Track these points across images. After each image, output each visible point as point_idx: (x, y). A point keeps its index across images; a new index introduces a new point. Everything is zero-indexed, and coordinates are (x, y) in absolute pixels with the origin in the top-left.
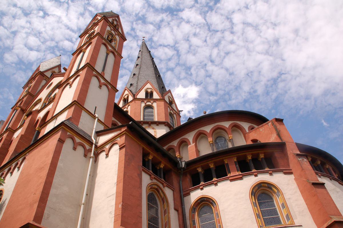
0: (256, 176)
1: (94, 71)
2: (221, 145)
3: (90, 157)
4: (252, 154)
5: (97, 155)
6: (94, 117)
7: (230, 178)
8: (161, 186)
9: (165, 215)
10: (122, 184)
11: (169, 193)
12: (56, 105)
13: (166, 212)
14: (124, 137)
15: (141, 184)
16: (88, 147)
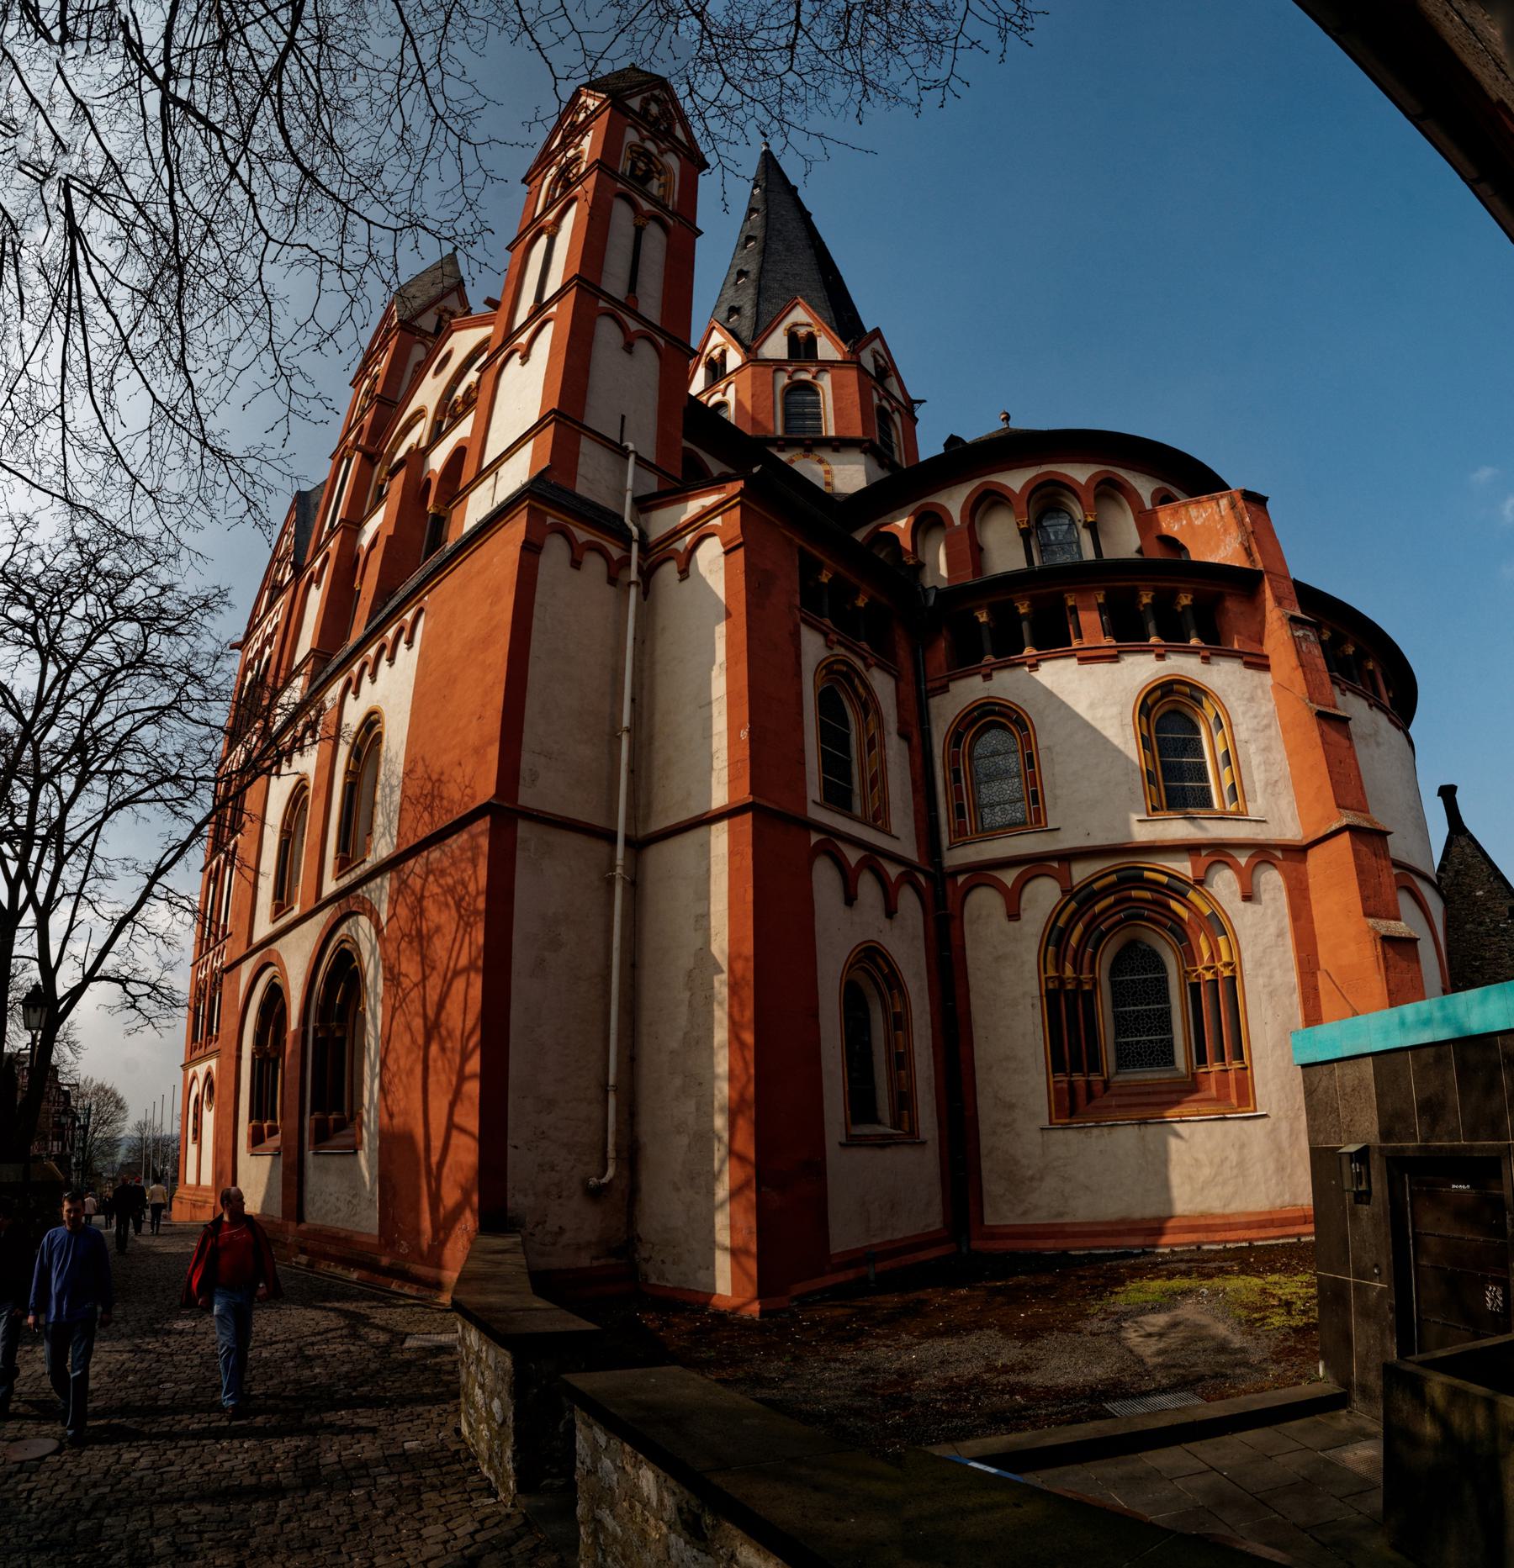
2: (1056, 537)
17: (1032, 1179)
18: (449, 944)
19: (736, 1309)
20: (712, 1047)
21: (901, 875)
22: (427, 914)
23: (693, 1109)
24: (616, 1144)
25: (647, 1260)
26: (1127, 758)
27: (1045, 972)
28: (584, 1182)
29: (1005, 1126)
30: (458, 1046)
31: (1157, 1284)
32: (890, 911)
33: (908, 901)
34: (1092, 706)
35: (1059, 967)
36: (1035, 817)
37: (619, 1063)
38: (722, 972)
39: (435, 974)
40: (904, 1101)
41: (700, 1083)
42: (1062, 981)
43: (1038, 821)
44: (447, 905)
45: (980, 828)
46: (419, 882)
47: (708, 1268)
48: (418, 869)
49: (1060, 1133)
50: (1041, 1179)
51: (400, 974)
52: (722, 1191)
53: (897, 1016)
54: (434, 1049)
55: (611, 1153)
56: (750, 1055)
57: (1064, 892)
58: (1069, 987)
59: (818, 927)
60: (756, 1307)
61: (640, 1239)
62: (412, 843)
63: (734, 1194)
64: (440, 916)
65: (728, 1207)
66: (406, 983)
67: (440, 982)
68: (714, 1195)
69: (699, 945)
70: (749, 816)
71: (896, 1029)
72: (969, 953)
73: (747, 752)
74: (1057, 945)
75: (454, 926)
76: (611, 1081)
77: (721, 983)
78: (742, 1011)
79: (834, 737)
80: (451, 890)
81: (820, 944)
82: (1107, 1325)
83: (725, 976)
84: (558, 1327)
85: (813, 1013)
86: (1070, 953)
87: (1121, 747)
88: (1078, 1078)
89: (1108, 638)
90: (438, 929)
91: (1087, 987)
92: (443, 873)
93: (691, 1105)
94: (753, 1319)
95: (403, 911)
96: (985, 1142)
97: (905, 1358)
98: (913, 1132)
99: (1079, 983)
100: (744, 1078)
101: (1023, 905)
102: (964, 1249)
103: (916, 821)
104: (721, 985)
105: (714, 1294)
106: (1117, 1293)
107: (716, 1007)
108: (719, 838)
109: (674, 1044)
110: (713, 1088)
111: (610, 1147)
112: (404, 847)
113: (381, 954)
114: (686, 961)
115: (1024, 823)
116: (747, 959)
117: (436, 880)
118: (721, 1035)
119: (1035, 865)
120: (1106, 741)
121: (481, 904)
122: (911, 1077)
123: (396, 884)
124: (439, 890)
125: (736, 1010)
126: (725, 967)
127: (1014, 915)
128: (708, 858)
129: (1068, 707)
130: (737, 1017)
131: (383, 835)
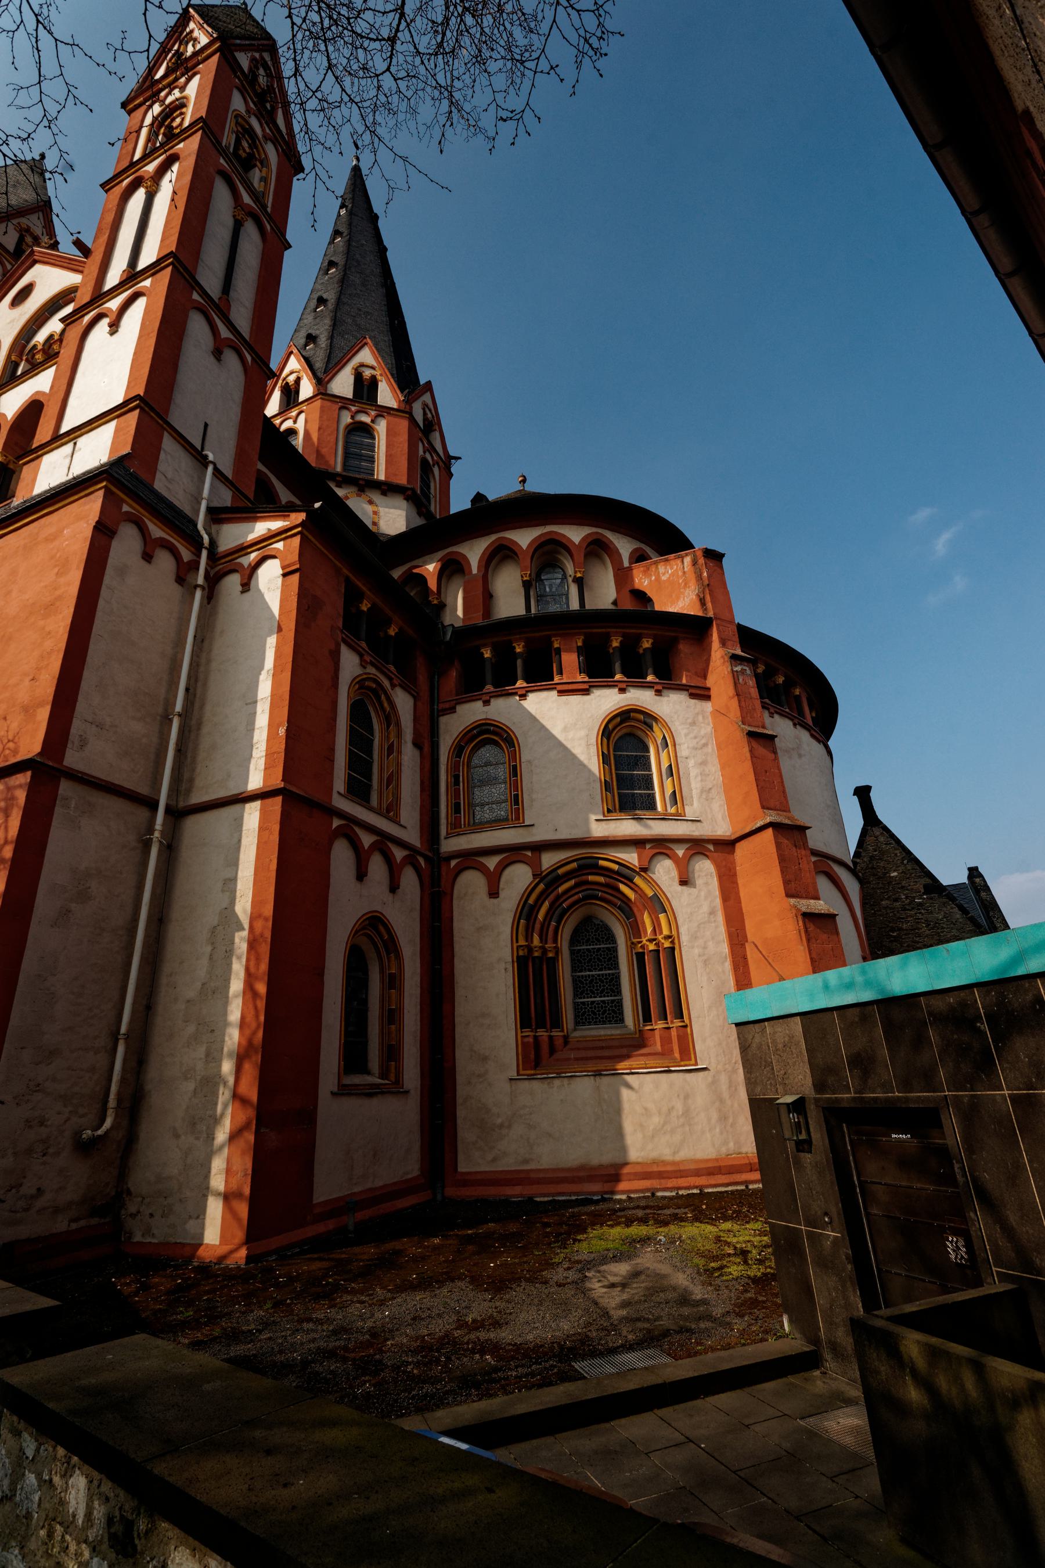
0: (622, 691)
1: (193, 288)
2: (551, 590)
3: (196, 586)
4: (624, 635)
5: (213, 581)
6: (202, 461)
7: (560, 687)
8: (386, 683)
9: (388, 756)
10: (287, 675)
11: (403, 702)
12: (64, 387)
13: (392, 750)
14: (297, 540)
15: (338, 678)
16: (186, 555)
17: (501, 1126)
19: (223, 1258)
20: (227, 997)
21: (405, 858)
24: (119, 1094)
25: (133, 1216)
26: (590, 771)
27: (517, 942)
28: (78, 1134)
29: (479, 1076)
31: (617, 1232)
33: (409, 879)
34: (565, 729)
35: (528, 937)
36: (515, 816)
37: (133, 1012)
38: (243, 929)
40: (392, 1053)
41: (214, 1029)
42: (530, 949)
43: (518, 818)
45: (472, 822)
49: (526, 1083)
50: (509, 1127)
52: (221, 1135)
53: (392, 977)
55: (112, 1102)
56: (261, 1004)
57: (535, 876)
58: (536, 954)
59: (331, 898)
60: (243, 1252)
61: (129, 1193)
63: (233, 1137)
65: (226, 1151)
68: (213, 1139)
69: (225, 905)
70: (279, 800)
71: (390, 988)
72: (456, 924)
73: (283, 746)
74: (528, 919)
76: (123, 1029)
77: (242, 939)
78: (257, 965)
79: (359, 740)
81: (332, 912)
82: (572, 1275)
83: (245, 934)
85: (319, 972)
86: (537, 926)
87: (586, 762)
88: (542, 1033)
91: (550, 955)
93: (201, 1051)
94: (239, 1267)
96: (461, 1091)
98: (398, 1082)
99: (545, 951)
100: (254, 1025)
101: (501, 886)
102: (439, 1197)
103: (421, 814)
104: (241, 942)
106: (580, 1241)
108: (252, 815)
109: (191, 993)
110: (224, 1035)
114: (211, 918)
115: (507, 819)
116: (266, 919)
118: (237, 985)
119: (513, 853)
120: (574, 757)
122: (400, 1031)
125: (252, 963)
126: (246, 926)
127: (494, 893)
128: (241, 831)
129: (547, 730)
130: (252, 970)
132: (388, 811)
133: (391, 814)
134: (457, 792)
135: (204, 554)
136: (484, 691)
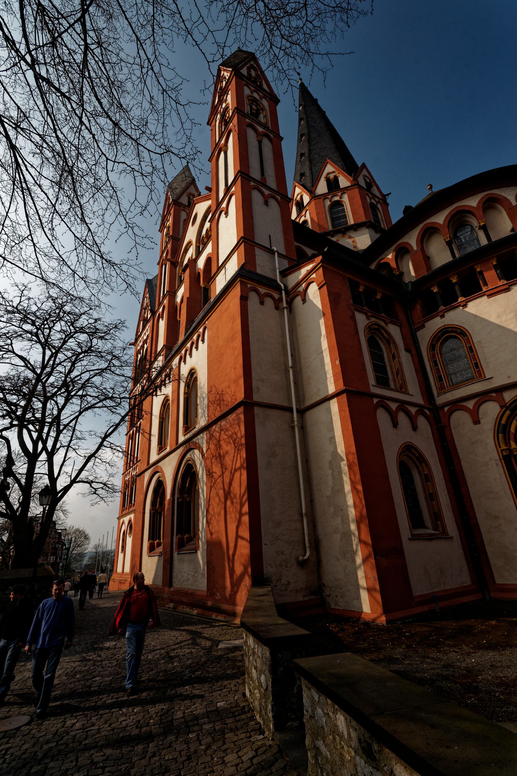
3: (284, 308)
5: (290, 303)
6: (272, 252)
7: (488, 293)
8: (383, 324)
9: (393, 361)
11: (394, 331)
14: (321, 270)
16: (276, 296)
18: (232, 458)
19: (374, 620)
20: (345, 493)
22: (222, 447)
23: (340, 522)
24: (309, 540)
25: (329, 596)
27: (500, 447)
28: (297, 558)
30: (239, 501)
32: (415, 428)
33: (422, 422)
34: (499, 316)
37: (306, 503)
38: (344, 460)
39: (227, 471)
41: (342, 509)
42: (511, 451)
43: (480, 376)
44: (230, 443)
45: (451, 384)
46: (218, 434)
47: (357, 599)
48: (217, 429)
51: (213, 472)
52: (359, 560)
53: (426, 475)
54: (229, 503)
55: (307, 545)
56: (362, 495)
57: (502, 407)
60: (383, 619)
61: (324, 586)
62: (214, 419)
63: (365, 561)
64: (227, 448)
65: (362, 567)
66: (215, 476)
67: (230, 474)
68: (355, 562)
69: (332, 450)
70: (345, 395)
72: (456, 443)
73: (340, 369)
74: (504, 433)
75: (233, 451)
76: (304, 512)
77: (344, 465)
78: (355, 476)
80: (231, 437)
84: (291, 633)
85: (386, 477)
86: (512, 437)
89: (502, 281)
90: (227, 452)
92: (227, 430)
93: (339, 520)
95: (212, 446)
96: (486, 538)
97: (468, 661)
100: (361, 506)
101: (480, 416)
103: (420, 387)
104: (344, 467)
105: (363, 612)
107: (344, 476)
108: (334, 405)
109: (328, 493)
110: (348, 512)
111: (307, 542)
112: (211, 421)
113: (204, 465)
115: (473, 378)
116: (353, 454)
117: (225, 433)
118: (347, 487)
120: (510, 331)
121: (243, 441)
122: (438, 504)
123: (208, 436)
124: (226, 437)
125: (352, 476)
126: (345, 458)
127: (477, 422)
129: (486, 320)
130: (353, 479)
131: (202, 417)
132: (401, 389)
133: (403, 390)
134: (438, 370)
135: (283, 292)
136: (439, 310)
